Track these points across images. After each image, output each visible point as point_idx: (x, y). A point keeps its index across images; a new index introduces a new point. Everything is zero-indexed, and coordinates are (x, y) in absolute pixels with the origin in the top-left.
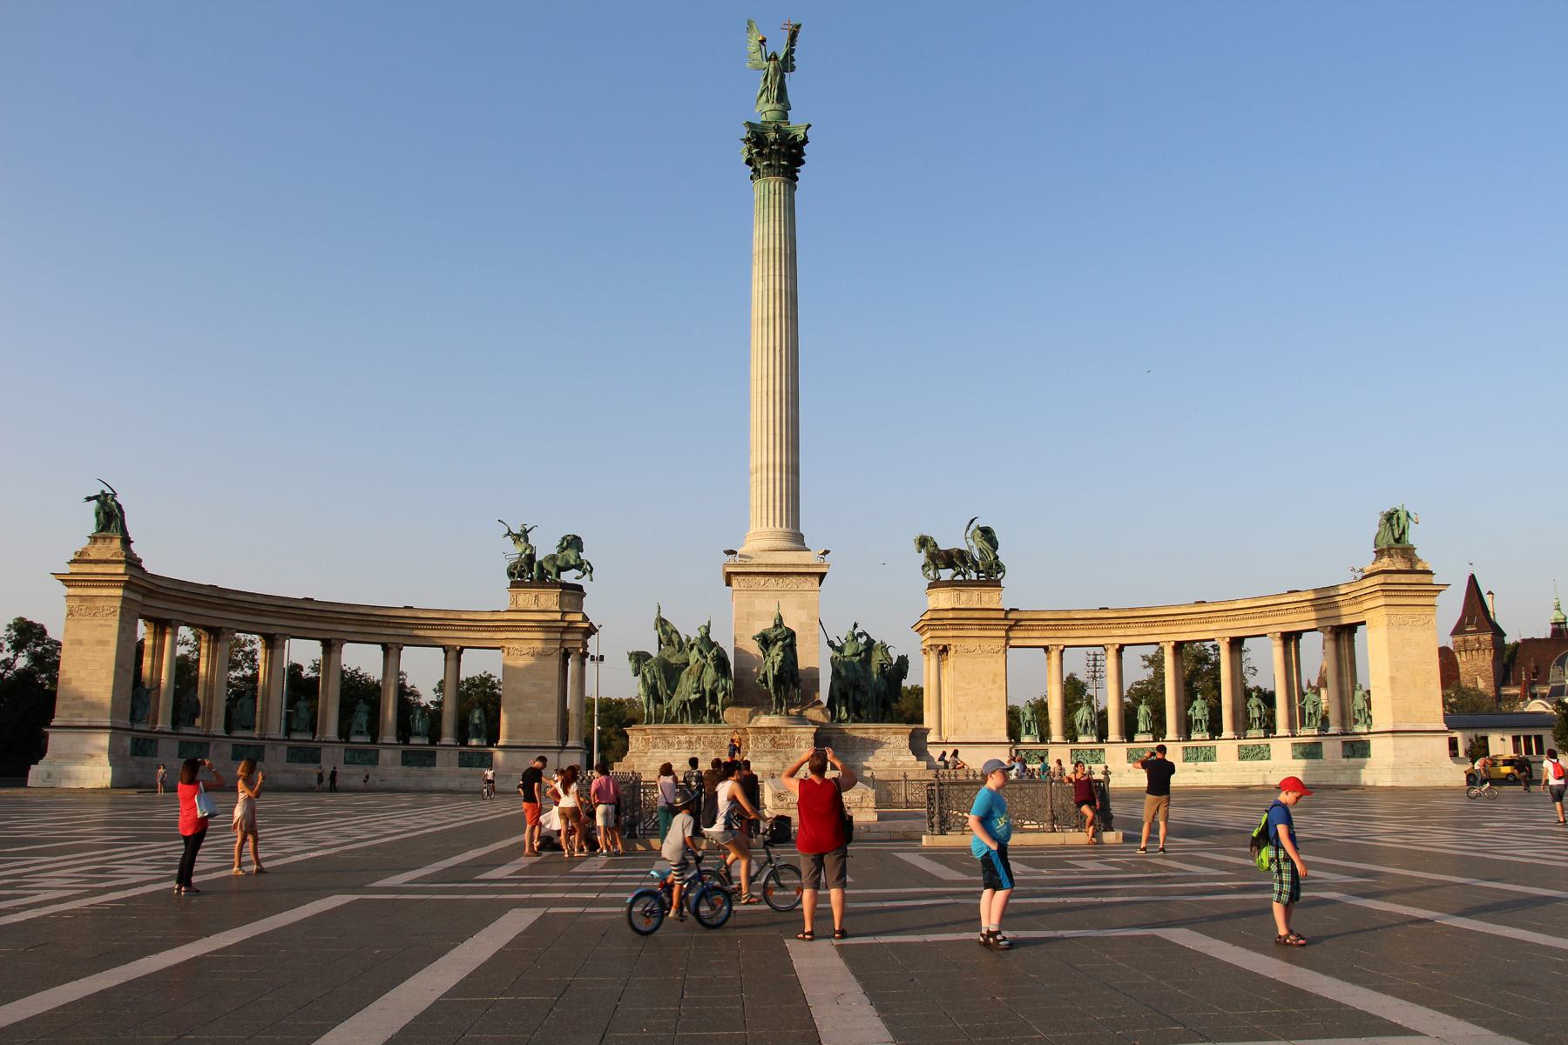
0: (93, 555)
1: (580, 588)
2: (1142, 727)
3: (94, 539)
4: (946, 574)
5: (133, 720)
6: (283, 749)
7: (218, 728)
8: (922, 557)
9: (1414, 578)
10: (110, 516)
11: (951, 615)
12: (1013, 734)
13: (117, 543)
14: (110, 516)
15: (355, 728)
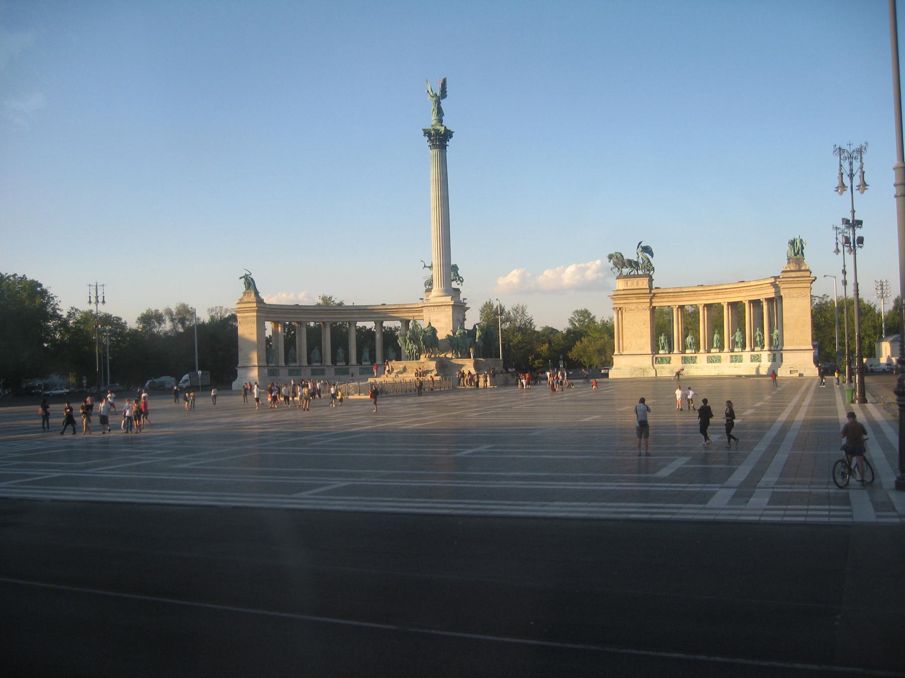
0: (245, 300)
1: (458, 290)
2: (715, 345)
3: (245, 294)
4: (626, 271)
5: (268, 361)
6: (332, 369)
7: (305, 363)
8: (611, 264)
9: (799, 274)
10: (250, 283)
11: (623, 292)
12: (655, 348)
13: (253, 294)
14: (250, 283)
15: (364, 358)
